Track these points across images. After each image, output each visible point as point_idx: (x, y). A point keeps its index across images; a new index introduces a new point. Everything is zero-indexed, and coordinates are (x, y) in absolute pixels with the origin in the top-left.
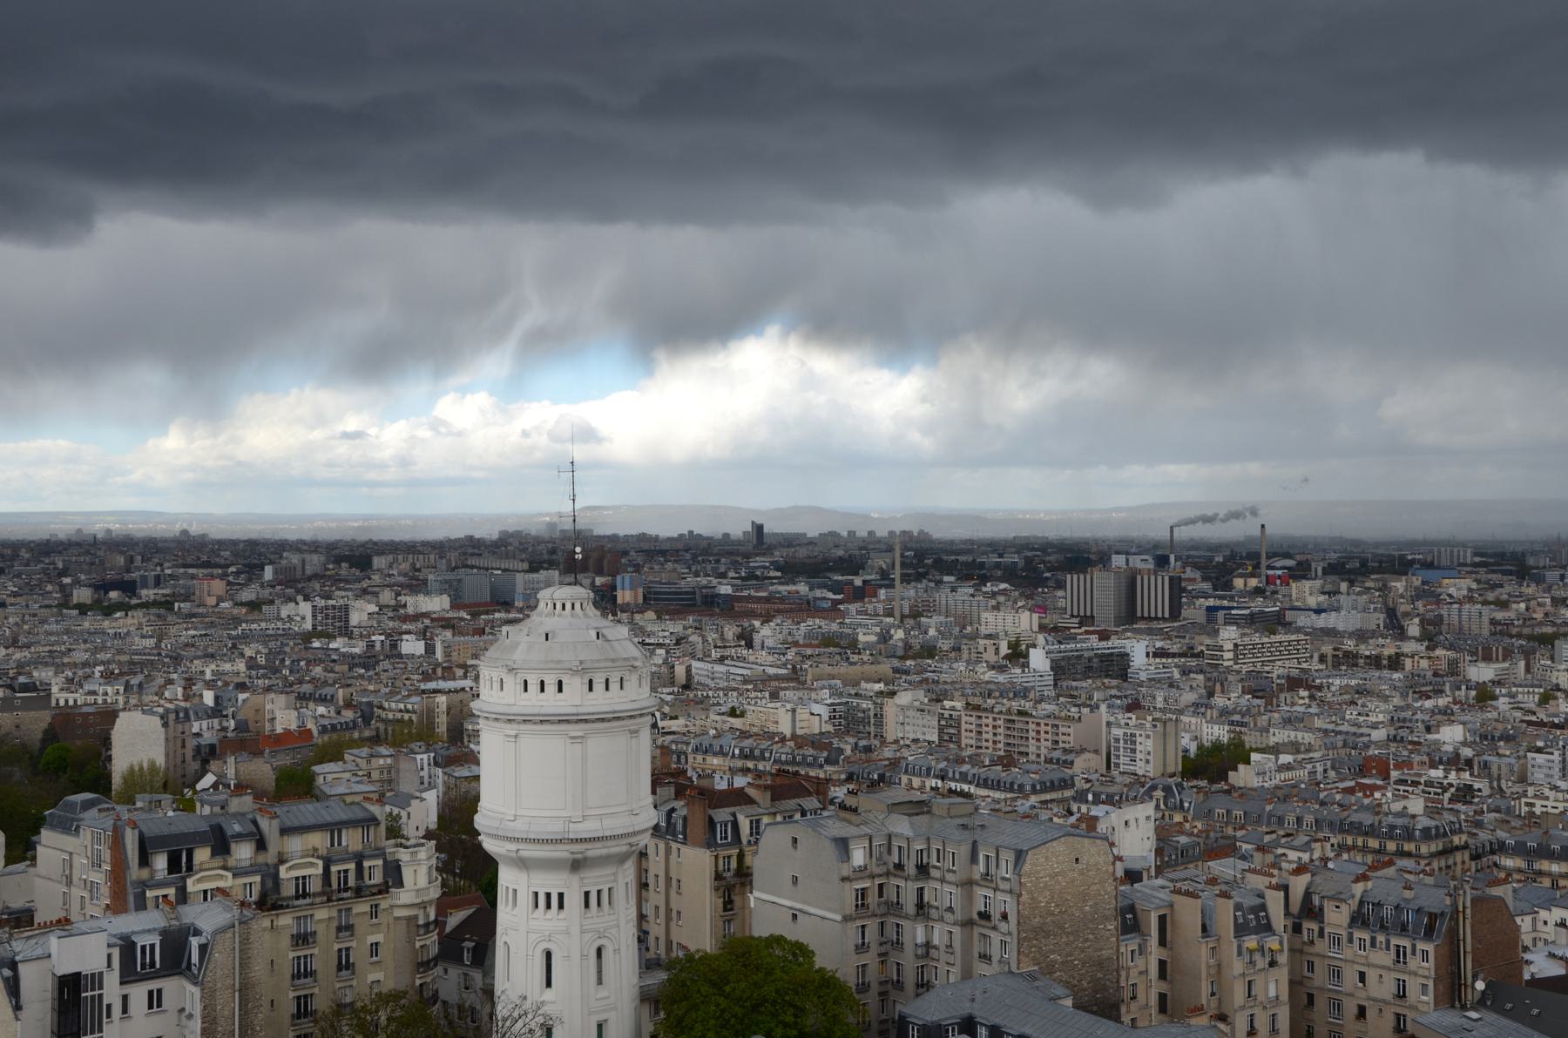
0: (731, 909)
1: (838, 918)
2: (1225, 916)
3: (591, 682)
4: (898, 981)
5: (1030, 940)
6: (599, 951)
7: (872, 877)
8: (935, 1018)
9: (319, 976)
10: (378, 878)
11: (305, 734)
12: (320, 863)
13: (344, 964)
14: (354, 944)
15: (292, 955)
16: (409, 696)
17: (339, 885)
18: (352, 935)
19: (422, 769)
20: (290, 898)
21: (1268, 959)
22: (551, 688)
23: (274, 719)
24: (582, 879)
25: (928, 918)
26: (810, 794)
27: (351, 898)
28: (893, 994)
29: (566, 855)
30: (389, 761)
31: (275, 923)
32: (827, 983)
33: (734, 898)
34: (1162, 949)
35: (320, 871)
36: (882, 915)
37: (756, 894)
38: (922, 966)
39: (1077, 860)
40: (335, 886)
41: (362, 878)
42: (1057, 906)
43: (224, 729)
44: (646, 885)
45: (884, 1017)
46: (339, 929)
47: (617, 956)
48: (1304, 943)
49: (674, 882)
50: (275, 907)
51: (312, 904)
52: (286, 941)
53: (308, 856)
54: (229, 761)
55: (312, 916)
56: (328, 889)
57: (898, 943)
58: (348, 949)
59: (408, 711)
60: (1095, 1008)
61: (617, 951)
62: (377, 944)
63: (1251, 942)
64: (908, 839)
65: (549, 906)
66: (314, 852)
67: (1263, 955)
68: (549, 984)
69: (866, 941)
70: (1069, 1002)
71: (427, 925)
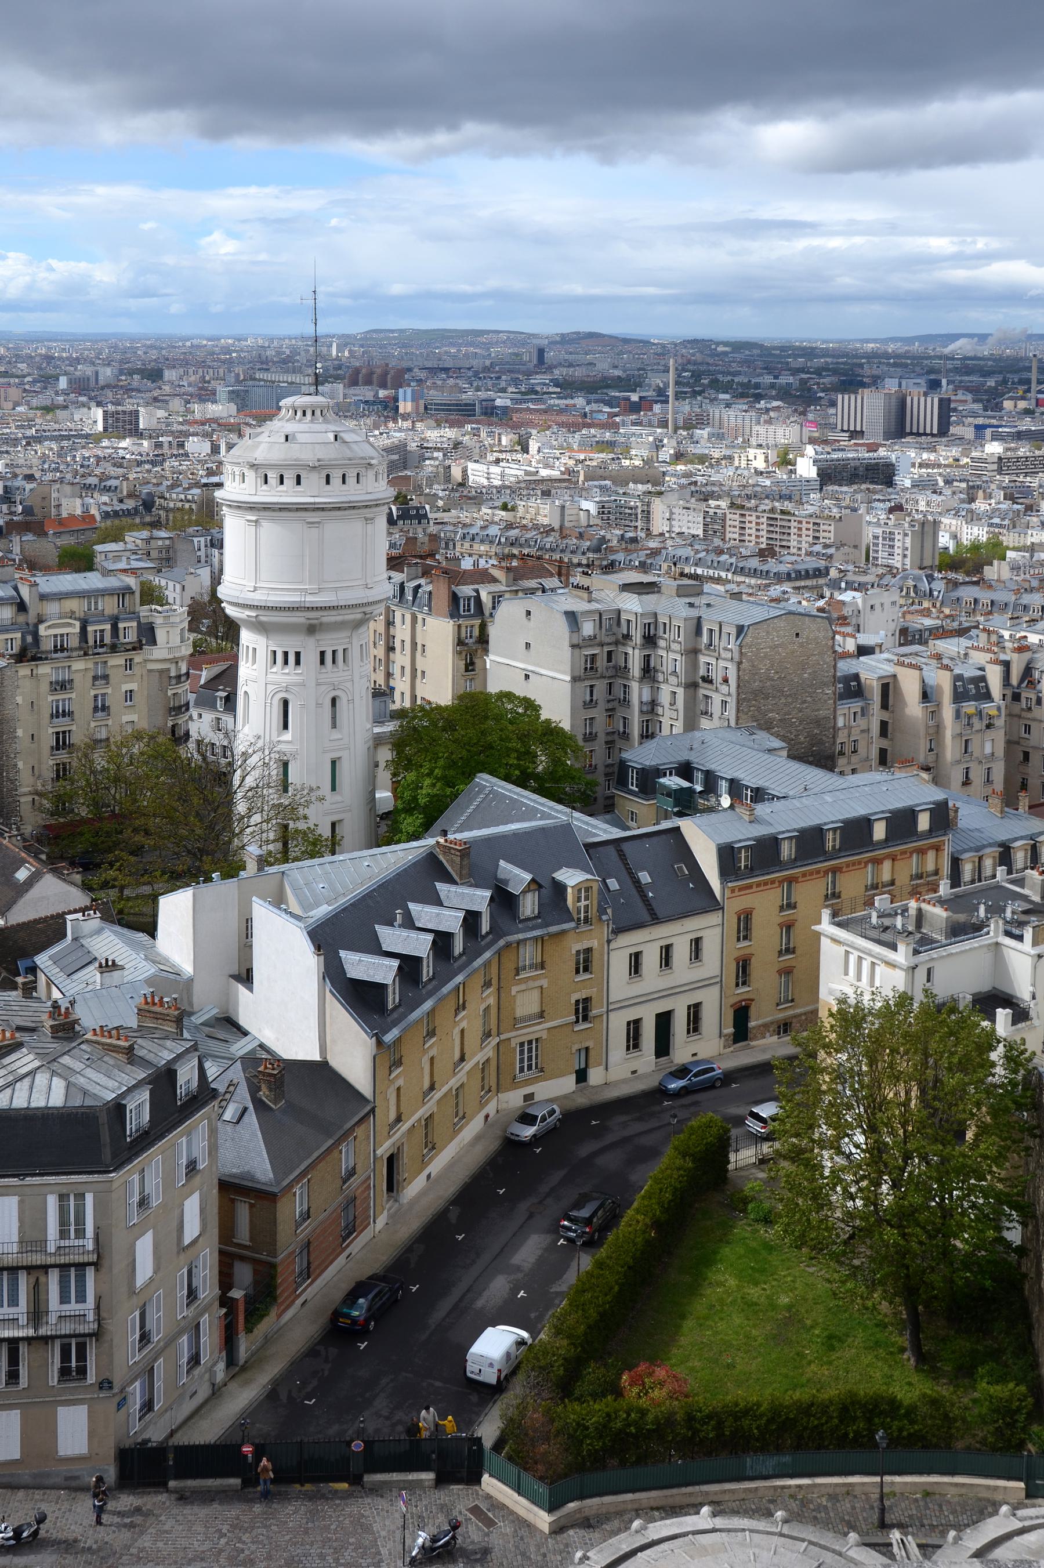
0: (473, 670)
2: (943, 681)
4: (624, 732)
5: (749, 700)
6: (334, 701)
8: (653, 763)
9: (76, 716)
10: (132, 637)
11: (87, 517)
12: (78, 624)
13: (101, 708)
14: (109, 691)
15: (50, 698)
16: (189, 489)
17: (96, 642)
18: (108, 683)
19: (199, 550)
20: (47, 652)
21: (986, 722)
23: (59, 506)
25: (654, 680)
27: (106, 653)
28: (620, 743)
30: (167, 542)
31: (35, 672)
32: (550, 733)
33: (476, 661)
34: (884, 712)
35: (77, 630)
36: (610, 677)
37: (492, 657)
38: (647, 721)
40: (91, 642)
41: (118, 637)
43: (12, 513)
44: (393, 649)
45: (610, 761)
46: (95, 678)
47: (351, 705)
48: (1023, 709)
49: (419, 647)
50: (34, 659)
51: (69, 657)
52: (45, 687)
53: (66, 618)
54: (13, 539)
55: (69, 667)
56: (85, 645)
57: (625, 700)
58: (104, 695)
59: (189, 501)
60: (811, 759)
62: (131, 691)
63: (970, 707)
66: (72, 615)
67: (981, 719)
69: (594, 698)
70: (785, 753)
71: (179, 677)
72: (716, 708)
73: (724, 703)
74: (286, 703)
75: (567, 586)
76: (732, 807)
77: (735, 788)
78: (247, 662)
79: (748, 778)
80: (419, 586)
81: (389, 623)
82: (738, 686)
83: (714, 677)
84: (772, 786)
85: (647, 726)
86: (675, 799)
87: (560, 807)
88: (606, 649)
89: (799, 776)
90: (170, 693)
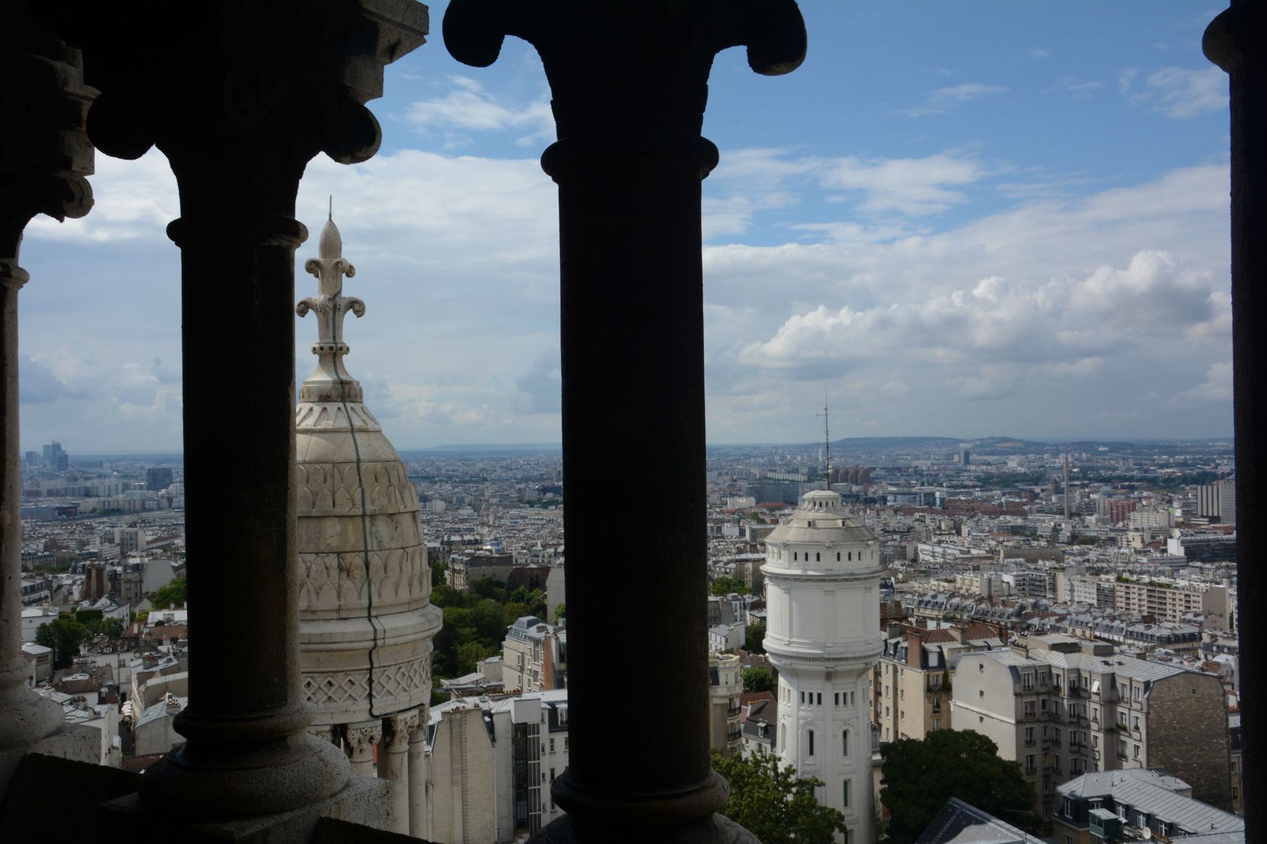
0: (939, 712)
1: (1013, 721)
3: (839, 554)
6: (845, 734)
7: (1038, 694)
22: (812, 558)
24: (833, 685)
26: (994, 636)
29: (822, 668)
36: (1045, 722)
39: (1194, 692)
42: (1178, 723)
45: (1046, 792)
49: (899, 692)
61: (857, 734)
64: (1063, 669)
65: (811, 702)
68: (811, 753)
72: (1129, 751)
73: (1137, 747)
74: (811, 734)
75: (1006, 645)
76: (1153, 839)
77: (1151, 820)
78: (784, 700)
79: (1161, 814)
80: (898, 643)
81: (877, 674)
82: (1148, 734)
83: (1127, 725)
84: (1183, 823)
85: (1075, 764)
86: (1105, 828)
87: (1015, 829)
88: (1041, 698)
89: (1205, 816)
90: (729, 722)
